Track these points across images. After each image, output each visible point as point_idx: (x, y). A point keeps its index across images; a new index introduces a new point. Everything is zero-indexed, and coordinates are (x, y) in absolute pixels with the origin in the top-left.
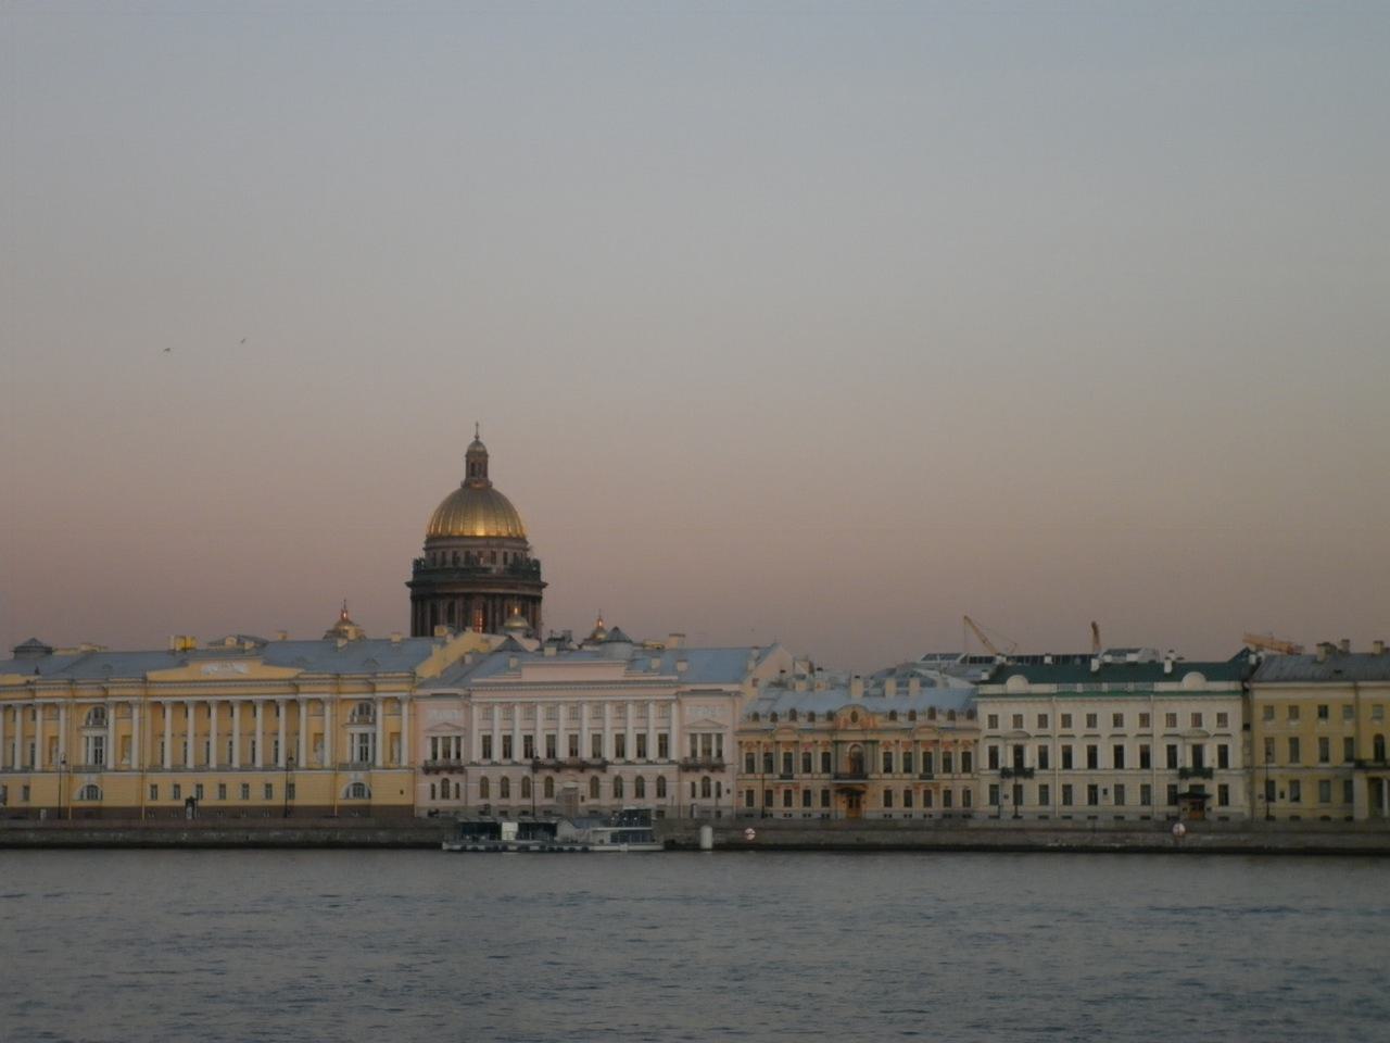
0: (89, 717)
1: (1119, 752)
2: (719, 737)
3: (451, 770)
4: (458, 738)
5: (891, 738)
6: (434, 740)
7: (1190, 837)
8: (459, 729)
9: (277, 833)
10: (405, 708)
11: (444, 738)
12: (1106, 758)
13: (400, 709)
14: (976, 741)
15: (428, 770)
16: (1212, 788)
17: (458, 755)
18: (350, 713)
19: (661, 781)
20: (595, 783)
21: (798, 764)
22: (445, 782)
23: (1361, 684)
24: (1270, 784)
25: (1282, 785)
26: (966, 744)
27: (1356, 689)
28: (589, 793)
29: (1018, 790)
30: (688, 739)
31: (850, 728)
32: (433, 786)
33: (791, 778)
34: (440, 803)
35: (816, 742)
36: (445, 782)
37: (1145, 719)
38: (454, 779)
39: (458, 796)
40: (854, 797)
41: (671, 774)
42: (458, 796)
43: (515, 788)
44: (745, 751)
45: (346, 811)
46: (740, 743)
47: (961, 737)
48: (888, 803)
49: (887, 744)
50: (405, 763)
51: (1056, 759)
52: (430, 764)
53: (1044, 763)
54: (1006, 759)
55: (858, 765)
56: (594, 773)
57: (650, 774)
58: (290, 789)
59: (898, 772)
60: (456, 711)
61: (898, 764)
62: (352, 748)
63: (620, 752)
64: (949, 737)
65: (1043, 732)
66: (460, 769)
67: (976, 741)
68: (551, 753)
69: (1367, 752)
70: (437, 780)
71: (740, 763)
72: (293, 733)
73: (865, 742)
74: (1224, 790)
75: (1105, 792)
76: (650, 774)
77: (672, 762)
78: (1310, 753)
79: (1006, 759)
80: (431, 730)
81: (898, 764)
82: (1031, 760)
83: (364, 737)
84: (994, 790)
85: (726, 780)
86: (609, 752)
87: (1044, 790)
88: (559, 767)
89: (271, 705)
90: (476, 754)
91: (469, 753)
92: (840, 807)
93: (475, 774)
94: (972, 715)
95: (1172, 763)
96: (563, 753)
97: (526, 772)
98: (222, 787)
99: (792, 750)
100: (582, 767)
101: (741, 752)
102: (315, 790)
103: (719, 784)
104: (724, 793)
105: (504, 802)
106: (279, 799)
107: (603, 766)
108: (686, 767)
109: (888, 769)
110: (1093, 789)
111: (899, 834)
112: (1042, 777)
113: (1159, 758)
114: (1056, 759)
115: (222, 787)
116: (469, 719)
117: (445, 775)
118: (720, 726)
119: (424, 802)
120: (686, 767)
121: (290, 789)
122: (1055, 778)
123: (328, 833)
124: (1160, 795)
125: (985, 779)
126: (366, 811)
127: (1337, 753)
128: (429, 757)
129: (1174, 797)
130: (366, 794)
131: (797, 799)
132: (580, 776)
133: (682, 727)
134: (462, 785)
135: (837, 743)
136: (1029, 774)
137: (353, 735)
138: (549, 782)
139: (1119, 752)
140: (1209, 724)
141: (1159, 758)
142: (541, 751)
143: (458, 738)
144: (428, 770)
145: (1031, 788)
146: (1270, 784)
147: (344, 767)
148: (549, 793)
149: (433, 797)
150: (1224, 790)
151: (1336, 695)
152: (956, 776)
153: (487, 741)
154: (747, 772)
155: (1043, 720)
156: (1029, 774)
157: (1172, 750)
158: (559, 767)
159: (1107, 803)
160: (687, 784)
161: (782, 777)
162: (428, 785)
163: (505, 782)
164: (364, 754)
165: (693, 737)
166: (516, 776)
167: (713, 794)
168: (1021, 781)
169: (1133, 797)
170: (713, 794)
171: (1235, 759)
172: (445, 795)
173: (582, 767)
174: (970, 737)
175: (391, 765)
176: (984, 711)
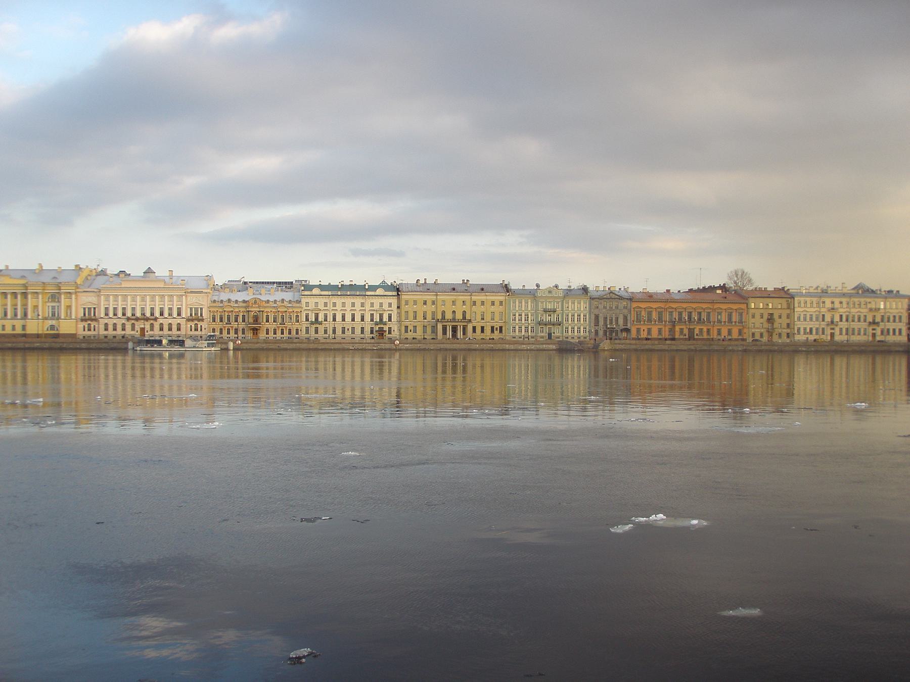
0: (49, 298)
1: (353, 316)
2: (201, 309)
3: (92, 320)
4: (95, 308)
5: (269, 310)
6: (84, 309)
7: (400, 345)
8: (95, 304)
9: (38, 344)
10: (74, 296)
11: (88, 308)
12: (348, 318)
13: (38, 296)
14: (301, 311)
15: (83, 320)
16: (386, 328)
17: (95, 315)
18: (47, 298)
20: (152, 326)
21: (232, 319)
22: (89, 325)
23: (438, 294)
24: (406, 327)
27: (437, 295)
31: (254, 306)
32: (84, 326)
33: (284, 324)
34: (87, 333)
35: (293, 311)
36: (89, 325)
37: (363, 305)
38: (93, 324)
39: (94, 330)
40: (255, 331)
41: (183, 322)
42: (94, 330)
43: (119, 327)
44: (212, 314)
45: (47, 336)
46: (210, 311)
47: (295, 310)
48: (267, 333)
49: (267, 312)
50: (73, 317)
51: (330, 318)
52: (83, 318)
53: (326, 320)
55: (256, 319)
56: (152, 322)
57: (174, 323)
58: (24, 327)
59: (271, 322)
60: (94, 298)
61: (271, 319)
62: (49, 312)
63: (162, 314)
64: (291, 310)
66: (96, 320)
67: (301, 311)
71: (210, 319)
72: (25, 306)
73: (260, 311)
74: (390, 328)
75: (348, 329)
76: (174, 323)
77: (184, 318)
78: (420, 317)
80: (83, 305)
81: (271, 319)
82: (321, 318)
83: (53, 307)
84: (307, 329)
85: (204, 325)
86: (157, 314)
88: (137, 319)
89: (15, 295)
90: (103, 315)
91: (100, 313)
92: (249, 335)
94: (299, 302)
95: (372, 320)
96: (138, 314)
98: (14, 326)
99: (230, 314)
100: (147, 319)
101: (210, 314)
102: (33, 327)
103: (201, 326)
104: (203, 329)
105: (115, 332)
106: (19, 330)
107: (156, 319)
108: (188, 320)
109: (267, 321)
110: (343, 329)
111: (294, 345)
112: (325, 324)
113: (367, 318)
114: (330, 318)
115: (14, 326)
116: (99, 301)
117: (89, 322)
118: (202, 305)
119: (81, 333)
120: (188, 320)
121: (24, 327)
122: (330, 325)
123: (61, 344)
124: (367, 330)
125: (304, 325)
126: (57, 336)
127: (429, 317)
128: (82, 315)
130: (56, 329)
131: (286, 332)
132: (146, 323)
133: (187, 305)
134: (96, 326)
135: (248, 311)
136: (321, 323)
137: (49, 306)
138: (133, 325)
139: (353, 316)
140: (386, 307)
141: (367, 318)
142: (129, 314)
143: (95, 308)
144: (83, 320)
145: (321, 329)
146: (406, 327)
147: (46, 319)
148: (133, 329)
149: (84, 330)
150: (390, 328)
151: (430, 297)
152: (263, 324)
153: (107, 309)
154: (243, 322)
155: (326, 304)
156: (321, 323)
157: (372, 315)
158: (137, 319)
159: (348, 333)
161: (226, 324)
162: (83, 326)
163: (115, 325)
164: (53, 314)
165: (191, 309)
166: (119, 323)
167: (199, 329)
168: (318, 326)
169: (358, 331)
170: (199, 329)
171: (394, 318)
172: (89, 330)
173: (147, 319)
175: (67, 318)
176: (304, 301)
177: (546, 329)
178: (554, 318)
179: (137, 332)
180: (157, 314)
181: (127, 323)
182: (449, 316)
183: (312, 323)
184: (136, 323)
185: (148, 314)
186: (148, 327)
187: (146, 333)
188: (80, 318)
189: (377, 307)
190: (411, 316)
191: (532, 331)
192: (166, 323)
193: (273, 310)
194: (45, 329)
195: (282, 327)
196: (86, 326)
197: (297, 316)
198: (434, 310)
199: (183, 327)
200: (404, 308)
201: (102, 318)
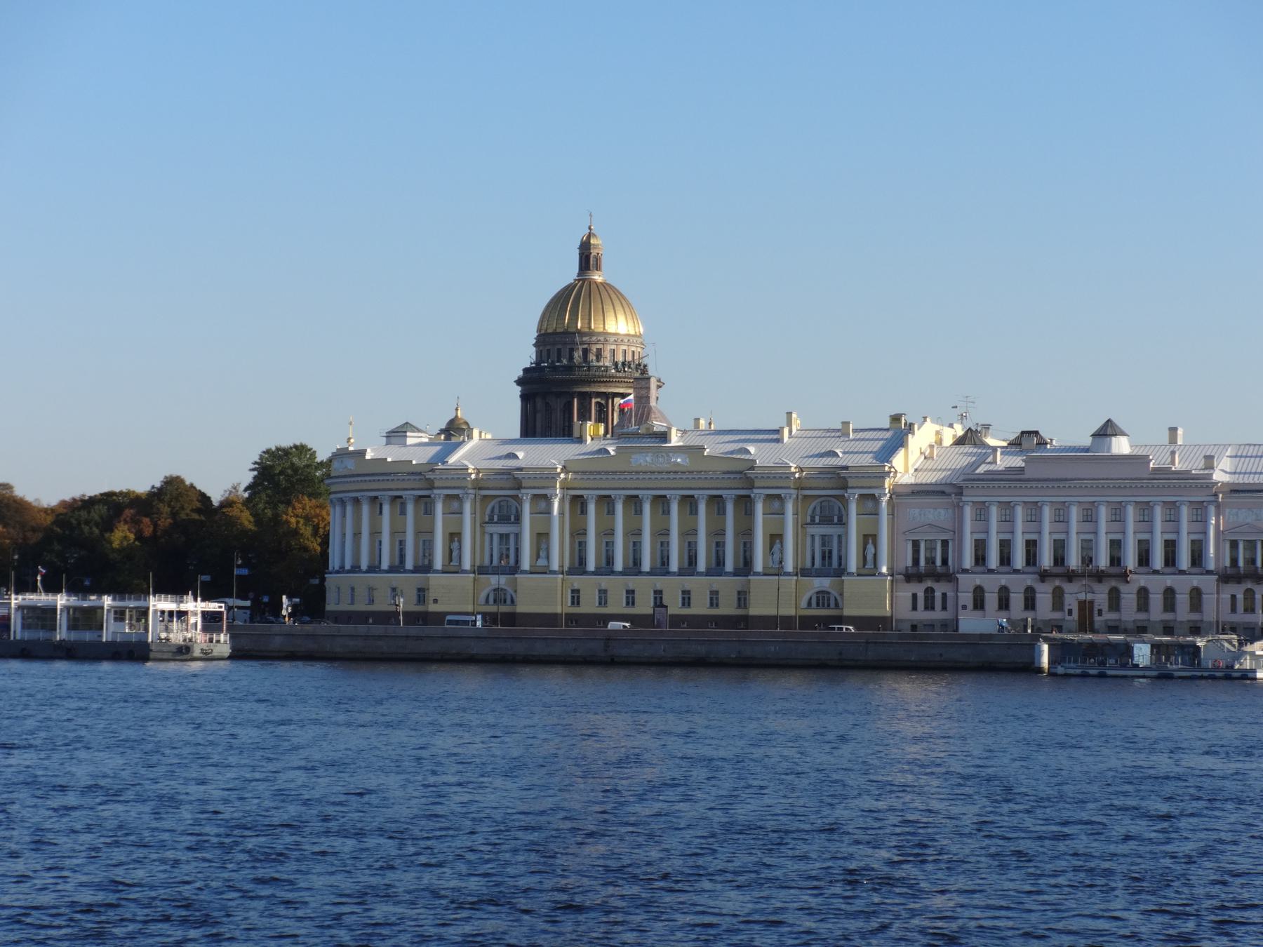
3: (938, 577)
4: (945, 543)
6: (916, 544)
8: (945, 530)
15: (911, 576)
17: (945, 561)
19: (1196, 594)
20: (1115, 600)
22: (929, 592)
28: (1107, 604)
30: (1228, 545)
34: (922, 615)
36: (929, 592)
38: (940, 589)
39: (944, 608)
41: (1207, 583)
56: (1114, 583)
57: (1183, 585)
58: (743, 598)
60: (943, 512)
63: (1144, 558)
66: (948, 576)
68: (1059, 560)
70: (919, 589)
72: (745, 535)
77: (1209, 572)
80: (910, 531)
83: (825, 539)
86: (1131, 561)
88: (1070, 576)
90: (968, 562)
93: (967, 583)
96: (1074, 561)
97: (1029, 580)
100: (1100, 576)
108: (1226, 578)
117: (929, 584)
120: (1226, 578)
128: (910, 563)
134: (950, 594)
138: (1058, 596)
142: (1046, 560)
143: (945, 543)
144: (911, 576)
149: (915, 608)
158: (1070, 576)
160: (1226, 597)
162: (910, 594)
165: (1234, 545)
166: (1018, 585)
172: (929, 606)
173: (1100, 576)
179: (1070, 612)
180: (1131, 561)
181: (1040, 587)
184: (1068, 587)
185: (1103, 562)
186: (1100, 596)
187: (1097, 618)
188: (904, 572)
192: (1156, 585)
194: (804, 603)
196: (921, 595)
199: (1209, 601)
201: (965, 571)
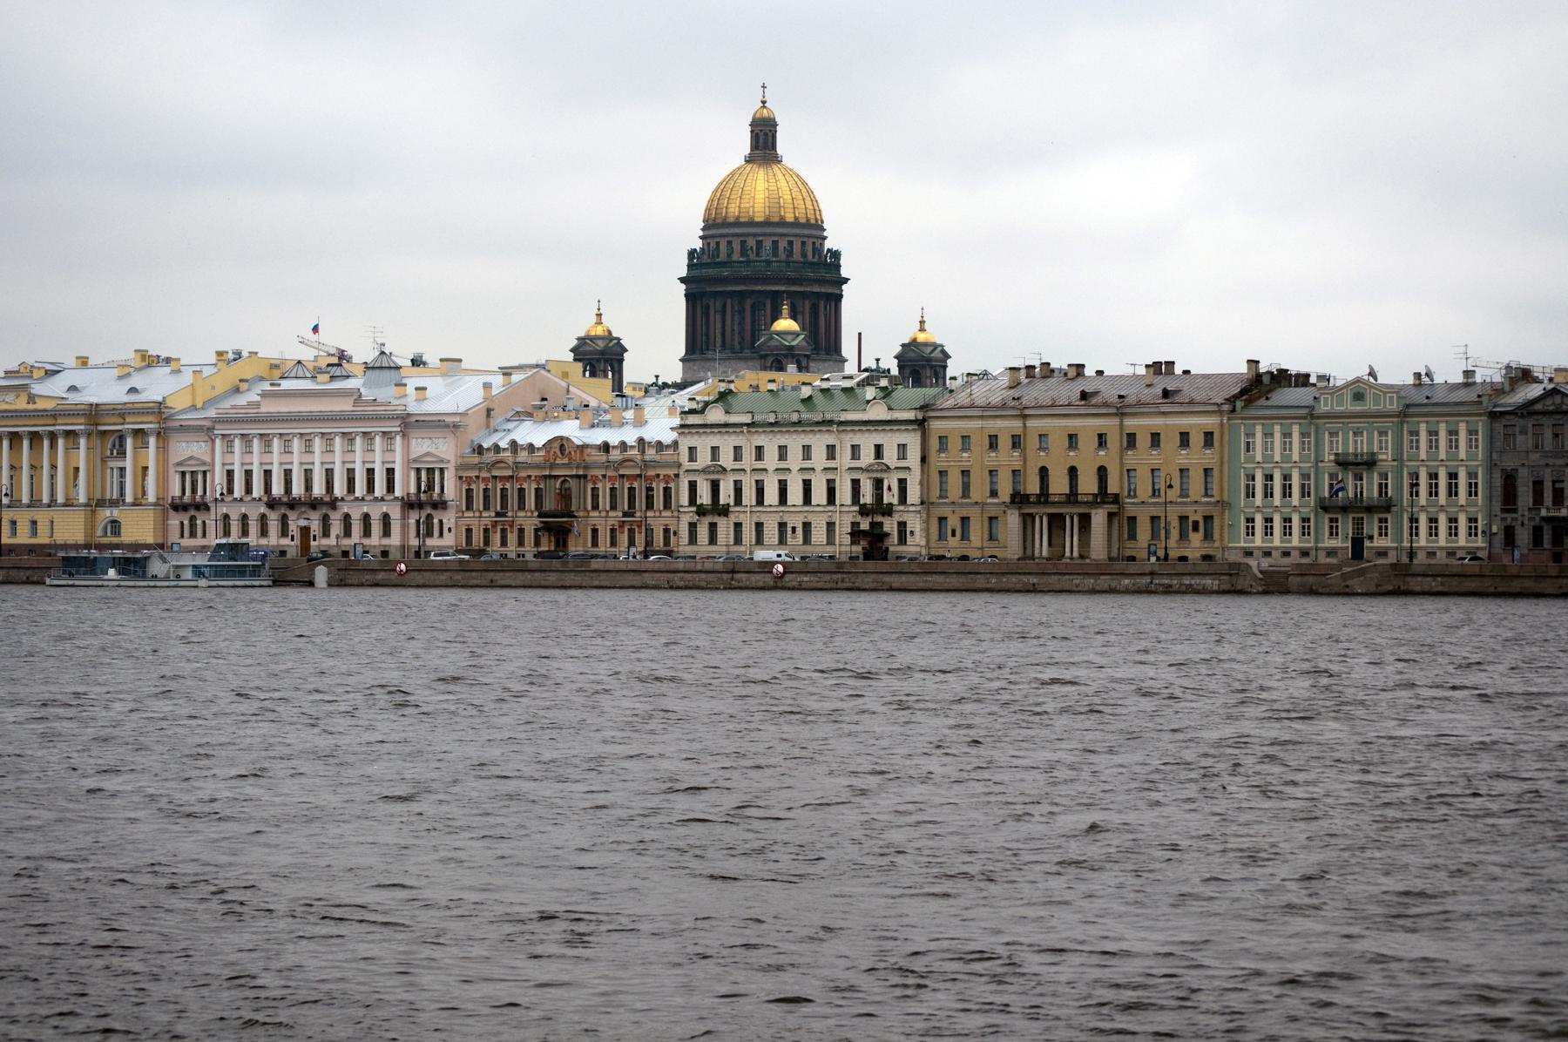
12: (795, 495)
16: (890, 525)
25: (954, 522)
26: (667, 478)
29: (713, 526)
47: (662, 472)
54: (704, 497)
65: (737, 465)
69: (1088, 485)
79: (704, 497)
82: (726, 495)
84: (693, 527)
87: (738, 526)
113: (844, 494)
129: (856, 534)
139: (807, 486)
140: (890, 457)
156: (724, 511)
168: (716, 519)
174: (672, 472)
177: (1347, 526)
178: (1370, 488)
182: (1059, 485)
183: (702, 511)
189: (867, 457)
190: (954, 488)
191: (1304, 532)
193: (611, 473)
195: (631, 523)
197: (667, 490)
198: (1017, 465)
200: (938, 461)
